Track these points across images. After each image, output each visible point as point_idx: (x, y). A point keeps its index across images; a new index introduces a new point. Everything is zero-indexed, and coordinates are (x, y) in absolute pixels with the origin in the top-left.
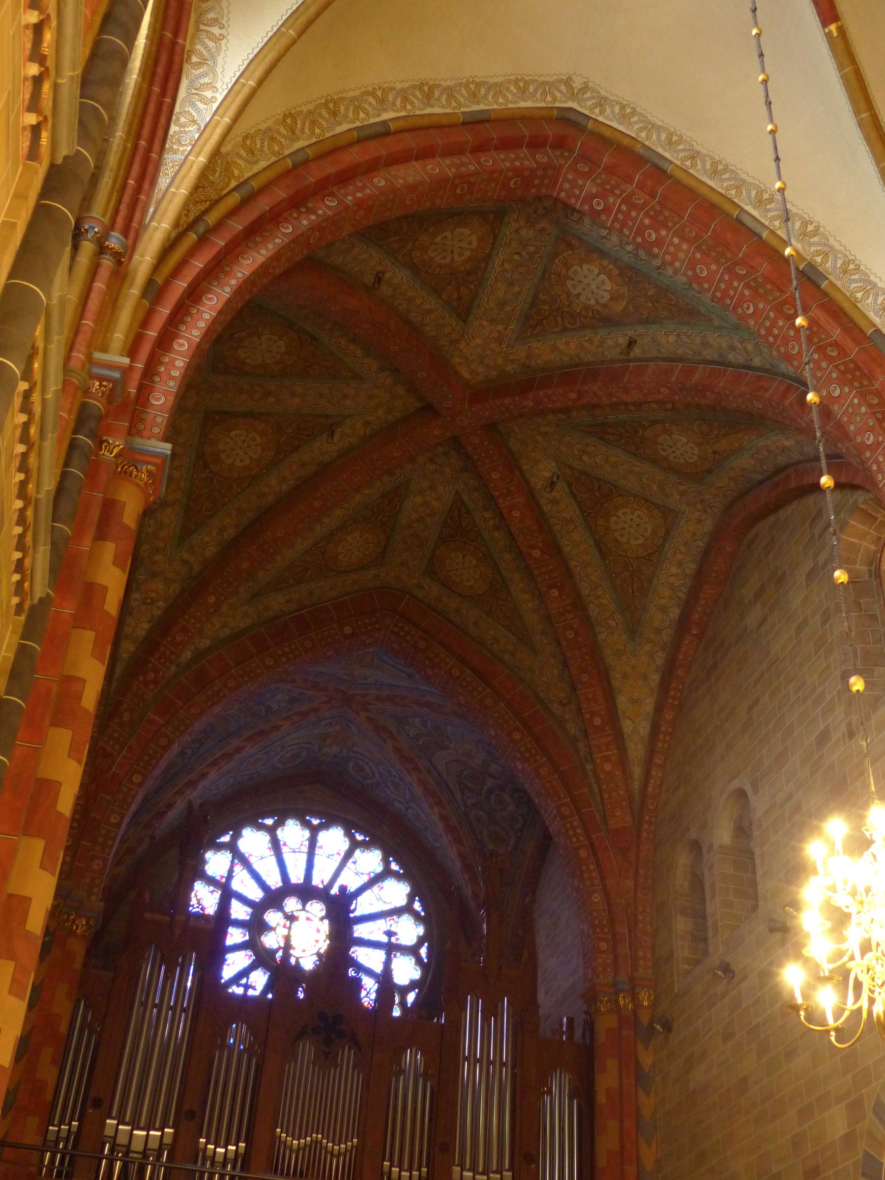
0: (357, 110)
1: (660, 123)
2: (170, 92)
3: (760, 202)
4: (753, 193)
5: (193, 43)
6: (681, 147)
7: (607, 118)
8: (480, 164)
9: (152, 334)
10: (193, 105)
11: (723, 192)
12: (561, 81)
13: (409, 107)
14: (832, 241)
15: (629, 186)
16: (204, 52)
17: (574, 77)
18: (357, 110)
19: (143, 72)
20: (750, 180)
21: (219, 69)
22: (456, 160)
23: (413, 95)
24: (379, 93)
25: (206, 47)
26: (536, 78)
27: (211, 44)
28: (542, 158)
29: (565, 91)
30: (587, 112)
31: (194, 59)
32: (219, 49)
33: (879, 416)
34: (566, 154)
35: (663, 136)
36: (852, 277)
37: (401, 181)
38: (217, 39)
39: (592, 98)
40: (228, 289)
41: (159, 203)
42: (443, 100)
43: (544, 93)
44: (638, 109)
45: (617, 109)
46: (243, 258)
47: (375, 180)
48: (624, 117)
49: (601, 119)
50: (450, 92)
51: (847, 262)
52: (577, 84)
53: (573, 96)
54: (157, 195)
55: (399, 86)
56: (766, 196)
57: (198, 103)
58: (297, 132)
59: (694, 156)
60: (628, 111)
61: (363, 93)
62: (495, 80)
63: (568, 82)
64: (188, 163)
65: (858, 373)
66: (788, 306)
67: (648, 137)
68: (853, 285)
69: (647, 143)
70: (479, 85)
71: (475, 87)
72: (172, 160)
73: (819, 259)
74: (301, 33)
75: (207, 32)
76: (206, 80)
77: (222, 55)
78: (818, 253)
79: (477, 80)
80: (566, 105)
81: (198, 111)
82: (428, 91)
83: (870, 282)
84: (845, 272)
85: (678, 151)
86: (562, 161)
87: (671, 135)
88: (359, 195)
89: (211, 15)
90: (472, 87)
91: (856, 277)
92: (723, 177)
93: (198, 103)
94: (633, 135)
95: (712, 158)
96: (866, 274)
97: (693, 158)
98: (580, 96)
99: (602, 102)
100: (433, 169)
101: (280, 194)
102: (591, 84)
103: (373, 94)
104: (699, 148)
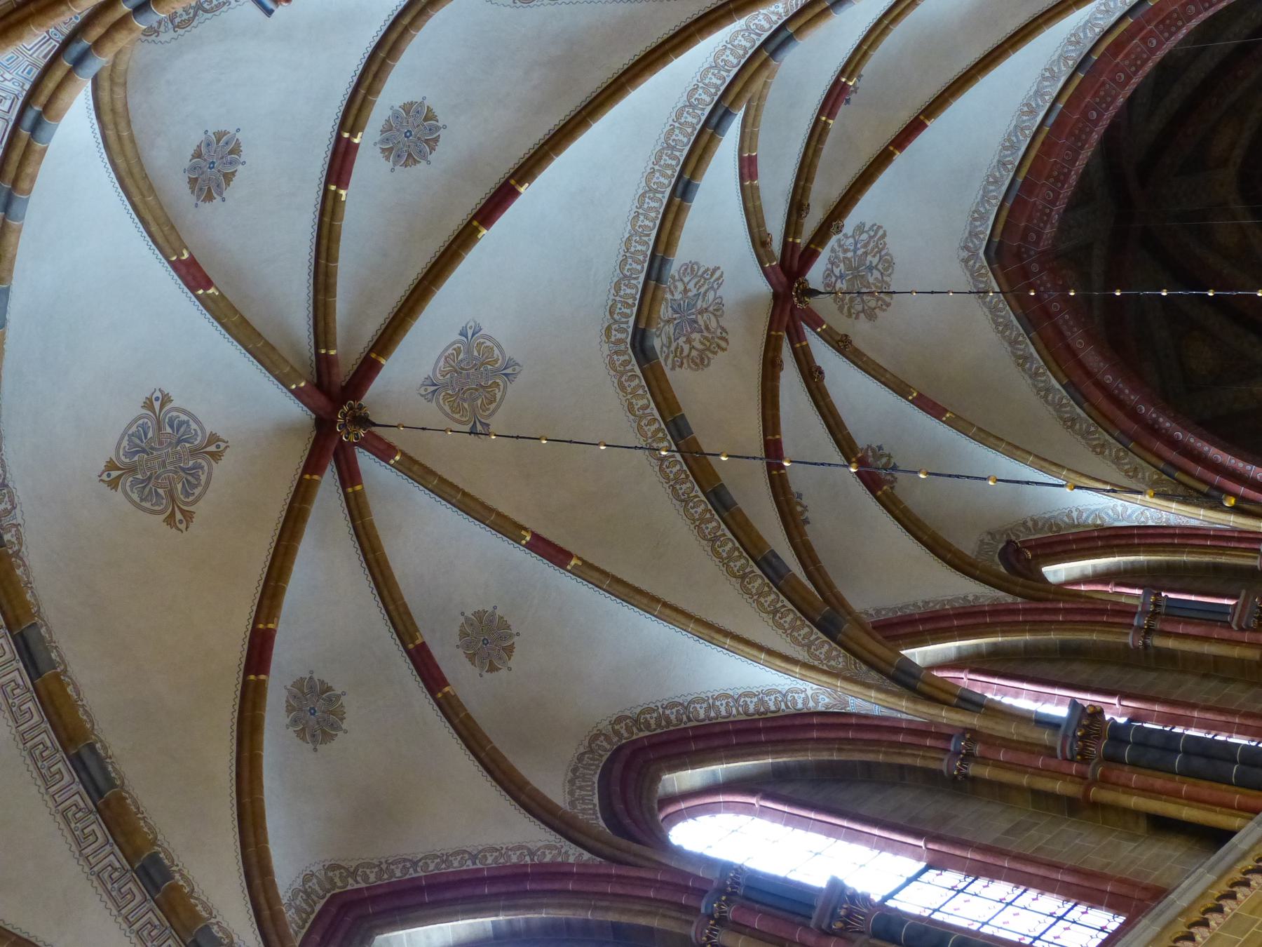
0: (1062, 406)
1: (981, 192)
2: (1130, 532)
3: (1031, 112)
4: (1025, 118)
5: (1089, 526)
6: (997, 174)
7: (986, 229)
8: (1061, 311)
10: (1130, 516)
11: (1029, 140)
12: (966, 266)
13: (1041, 371)
14: (1055, 57)
15: (1038, 203)
16: (1092, 517)
17: (961, 258)
18: (1062, 406)
19: (1136, 553)
20: (1014, 123)
21: (1100, 507)
22: (1064, 328)
23: (1030, 369)
24: (1043, 393)
25: (1088, 517)
26: (971, 284)
27: (1085, 515)
28: (1035, 268)
29: (972, 261)
30: (985, 243)
31: (1099, 522)
32: (1087, 510)
33: (1207, 5)
34: (1023, 250)
35: (992, 188)
36: (1082, 37)
37: (1102, 364)
38: (1080, 512)
39: (972, 242)
40: (1249, 467)
41: (1214, 523)
42: (1023, 347)
43: (981, 275)
44: (973, 209)
45: (978, 223)
46: (1217, 460)
47: (1108, 382)
48: (983, 217)
49: (988, 232)
50: (1013, 343)
51: (1070, 43)
52: (965, 254)
53: (974, 255)
54: (1206, 525)
55: (1029, 381)
56: (1026, 109)
57: (1128, 513)
58: (1102, 443)
59: (1002, 164)
60: (976, 215)
61: (1049, 404)
62: (988, 313)
63: (966, 261)
64: (1176, 512)
65: (1168, 22)
66: (1117, 78)
67: (996, 198)
68: (1089, 35)
69: (1001, 198)
70: (997, 324)
71: (1002, 327)
72: (1174, 520)
73: (1071, 63)
74: (1063, 467)
75: (1077, 519)
76: (1110, 512)
77: (1089, 507)
78: (1066, 64)
79: (994, 326)
80: (983, 258)
81: (1133, 512)
83: (1086, 24)
84: (1078, 43)
85: (1002, 176)
86: (1032, 253)
87: (989, 183)
88: (1127, 391)
89: (1066, 519)
90: (1000, 328)
91: (1082, 35)
92: (1015, 141)
93: (1128, 513)
94: (996, 208)
95: (1001, 151)
96: (1079, 28)
97: (1004, 164)
98: (973, 250)
99: (973, 234)
100: (1080, 343)
101: (1158, 446)
102: (962, 244)
103: (1045, 397)
104: (995, 161)
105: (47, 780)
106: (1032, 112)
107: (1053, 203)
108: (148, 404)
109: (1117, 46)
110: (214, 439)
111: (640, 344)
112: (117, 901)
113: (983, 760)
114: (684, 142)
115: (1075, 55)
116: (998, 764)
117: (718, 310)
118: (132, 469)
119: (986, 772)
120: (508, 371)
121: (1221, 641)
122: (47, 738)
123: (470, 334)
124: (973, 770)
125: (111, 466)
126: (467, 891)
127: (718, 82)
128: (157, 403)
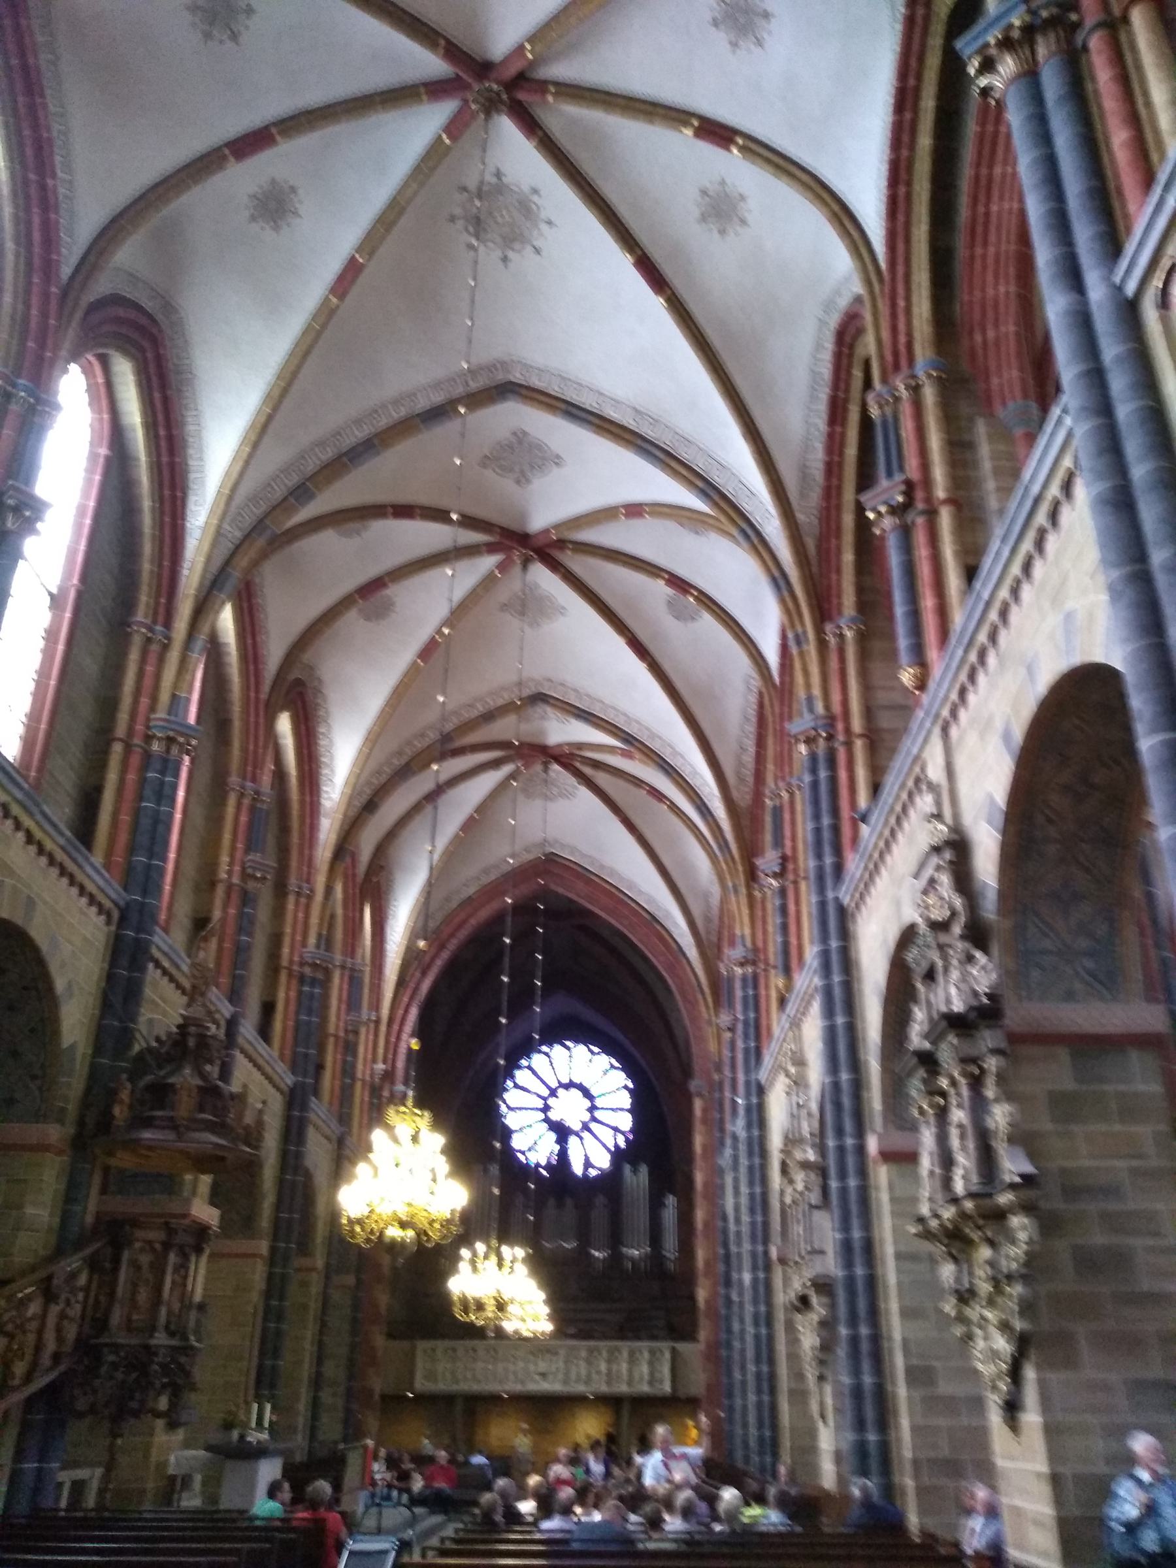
9: (393, 1040)
48: (572, 853)
59: (602, 867)
82: (486, 871)
99: (563, 846)
105: (358, 422)
106: (630, 888)
107: (578, 895)
108: (558, 457)
109: (661, 939)
110: (528, 481)
111: (540, 698)
112: (286, 470)
113: (297, 904)
114: (655, 745)
115: (659, 915)
116: (296, 911)
117: (543, 718)
118: (520, 442)
119: (290, 906)
120: (535, 624)
121: (339, 1009)
122: (383, 422)
123: (562, 611)
124: (291, 899)
125: (525, 433)
126: (248, 629)
127: (686, 773)
128: (558, 461)
